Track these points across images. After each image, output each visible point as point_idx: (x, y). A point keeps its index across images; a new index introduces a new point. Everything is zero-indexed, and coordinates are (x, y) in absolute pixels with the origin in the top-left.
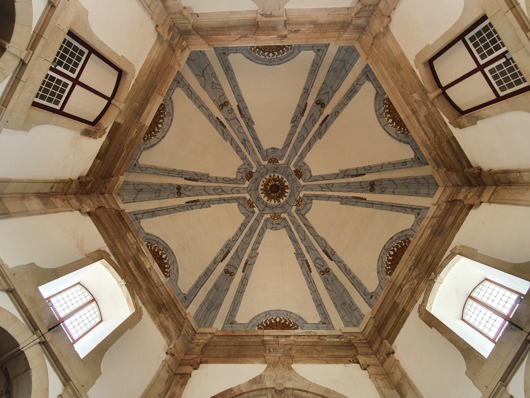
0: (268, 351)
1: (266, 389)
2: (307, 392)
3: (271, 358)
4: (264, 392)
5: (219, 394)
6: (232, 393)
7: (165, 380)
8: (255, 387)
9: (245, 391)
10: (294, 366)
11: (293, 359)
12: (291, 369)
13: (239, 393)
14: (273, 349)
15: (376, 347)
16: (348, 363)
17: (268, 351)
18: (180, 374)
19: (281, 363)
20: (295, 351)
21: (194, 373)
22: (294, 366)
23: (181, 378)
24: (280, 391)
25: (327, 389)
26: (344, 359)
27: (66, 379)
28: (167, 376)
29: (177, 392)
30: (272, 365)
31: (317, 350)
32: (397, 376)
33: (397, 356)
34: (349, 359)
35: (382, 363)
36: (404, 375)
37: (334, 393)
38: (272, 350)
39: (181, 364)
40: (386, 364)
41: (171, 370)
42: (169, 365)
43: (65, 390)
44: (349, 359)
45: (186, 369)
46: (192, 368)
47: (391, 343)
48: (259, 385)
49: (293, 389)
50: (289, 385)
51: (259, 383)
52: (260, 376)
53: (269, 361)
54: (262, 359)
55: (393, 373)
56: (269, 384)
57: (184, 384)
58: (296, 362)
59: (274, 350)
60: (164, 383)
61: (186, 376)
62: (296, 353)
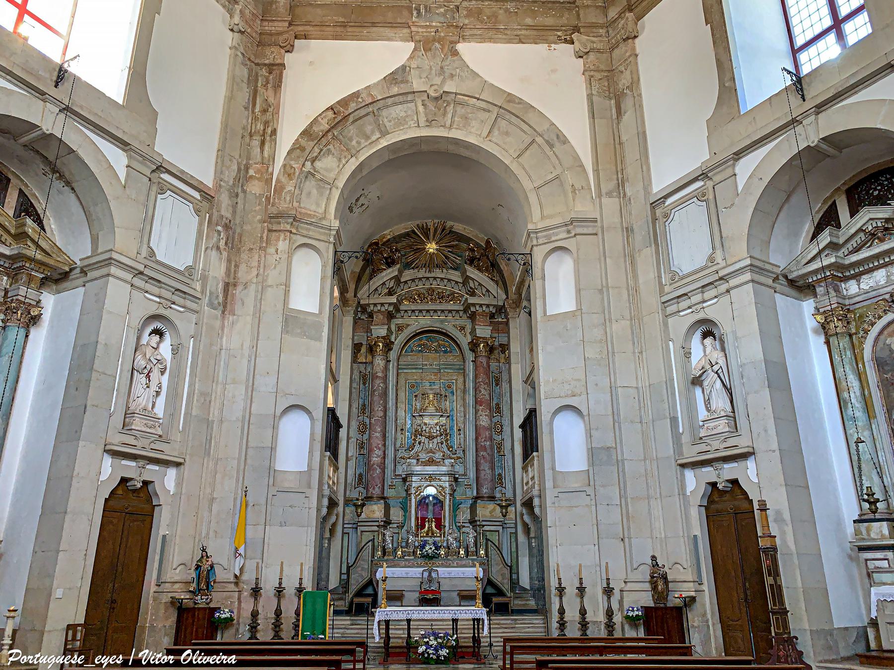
0: (415, 13)
1: (414, 92)
2: (478, 99)
3: (420, 30)
4: (410, 97)
5: (338, 102)
6: (360, 100)
7: (245, 80)
8: (395, 90)
9: (379, 98)
10: (461, 47)
11: (461, 33)
12: (455, 53)
13: (370, 101)
14: (426, 7)
15: (613, 13)
16: (555, 43)
17: (415, 13)
18: (265, 65)
19: (439, 43)
20: (465, 13)
21: (288, 58)
22: (461, 47)
23: (270, 73)
24: (436, 99)
25: (509, 94)
26: (550, 33)
27: (123, 144)
28: (246, 72)
29: (271, 100)
30: (425, 45)
31: (507, 10)
32: (624, 81)
33: (639, 44)
34: (559, 33)
35: (612, 49)
36: (635, 83)
37: (519, 103)
38: (423, 11)
39: (263, 41)
40: (616, 52)
41: (249, 59)
42: (243, 54)
43: (130, 157)
44: (559, 33)
45: (271, 55)
46: (283, 51)
47: (639, 18)
48: (402, 86)
49: (456, 94)
50: (450, 87)
51: (402, 82)
52: (403, 67)
53: (417, 38)
54: (406, 31)
55: (622, 72)
56: (417, 84)
57: (278, 86)
58: (464, 39)
59: (426, 11)
60: (245, 85)
61: (276, 69)
62: (467, 16)
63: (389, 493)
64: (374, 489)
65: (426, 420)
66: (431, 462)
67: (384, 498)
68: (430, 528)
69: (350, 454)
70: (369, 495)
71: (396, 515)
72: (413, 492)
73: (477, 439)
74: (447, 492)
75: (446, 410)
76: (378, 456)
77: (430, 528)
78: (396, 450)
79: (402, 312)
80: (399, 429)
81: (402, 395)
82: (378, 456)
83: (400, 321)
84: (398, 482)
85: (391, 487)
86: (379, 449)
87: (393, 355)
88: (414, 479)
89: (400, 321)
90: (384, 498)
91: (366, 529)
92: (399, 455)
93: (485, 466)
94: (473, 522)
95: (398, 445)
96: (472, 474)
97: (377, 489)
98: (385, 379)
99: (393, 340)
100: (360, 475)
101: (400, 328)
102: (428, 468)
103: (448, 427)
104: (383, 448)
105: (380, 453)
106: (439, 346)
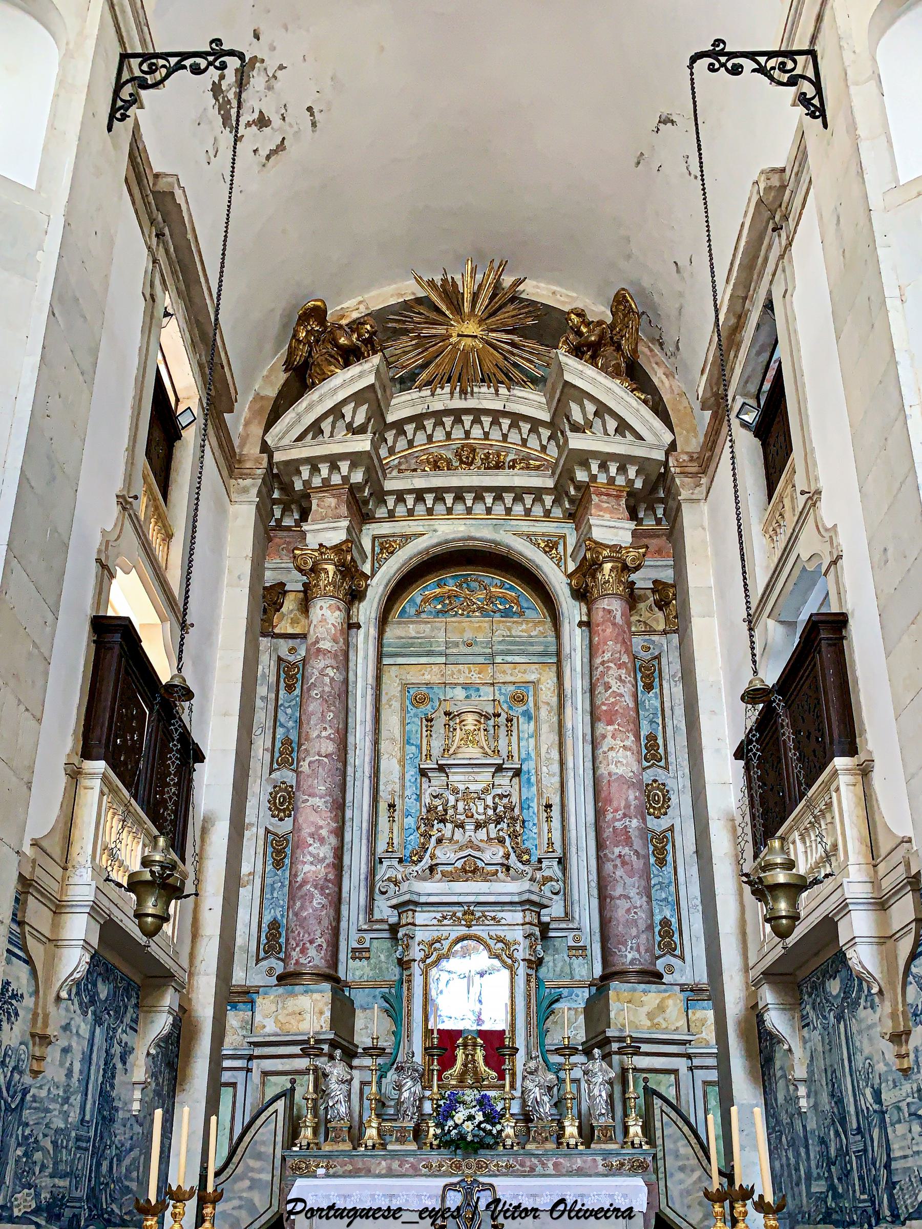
63: (352, 970)
64: (303, 951)
65: (457, 778)
66: (471, 871)
67: (333, 979)
68: (470, 1061)
69: (246, 869)
70: (291, 968)
71: (370, 1026)
72: (419, 956)
73: (599, 814)
74: (519, 955)
75: (510, 756)
76: (318, 860)
77: (470, 1061)
78: (374, 861)
79: (391, 501)
80: (383, 806)
81: (391, 721)
82: (318, 860)
83: (385, 529)
84: (381, 949)
85: (359, 953)
86: (322, 840)
87: (367, 610)
88: (421, 917)
89: (385, 529)
90: (333, 979)
91: (269, 1065)
92: (383, 872)
93: (626, 887)
94: (598, 1042)
95: (381, 847)
96: (587, 915)
97: (312, 952)
98: (344, 659)
99: (367, 569)
100: (274, 925)
101: (386, 546)
102: (460, 886)
103: (515, 799)
104: (333, 841)
105: (325, 851)
106: (491, 599)
